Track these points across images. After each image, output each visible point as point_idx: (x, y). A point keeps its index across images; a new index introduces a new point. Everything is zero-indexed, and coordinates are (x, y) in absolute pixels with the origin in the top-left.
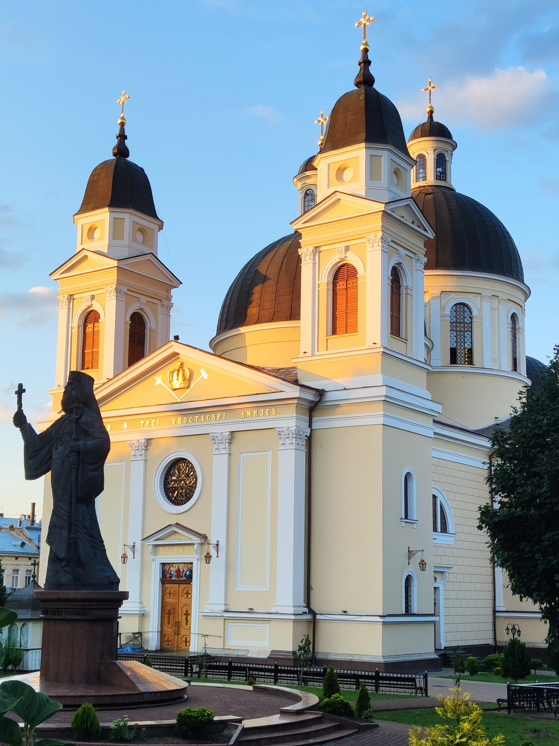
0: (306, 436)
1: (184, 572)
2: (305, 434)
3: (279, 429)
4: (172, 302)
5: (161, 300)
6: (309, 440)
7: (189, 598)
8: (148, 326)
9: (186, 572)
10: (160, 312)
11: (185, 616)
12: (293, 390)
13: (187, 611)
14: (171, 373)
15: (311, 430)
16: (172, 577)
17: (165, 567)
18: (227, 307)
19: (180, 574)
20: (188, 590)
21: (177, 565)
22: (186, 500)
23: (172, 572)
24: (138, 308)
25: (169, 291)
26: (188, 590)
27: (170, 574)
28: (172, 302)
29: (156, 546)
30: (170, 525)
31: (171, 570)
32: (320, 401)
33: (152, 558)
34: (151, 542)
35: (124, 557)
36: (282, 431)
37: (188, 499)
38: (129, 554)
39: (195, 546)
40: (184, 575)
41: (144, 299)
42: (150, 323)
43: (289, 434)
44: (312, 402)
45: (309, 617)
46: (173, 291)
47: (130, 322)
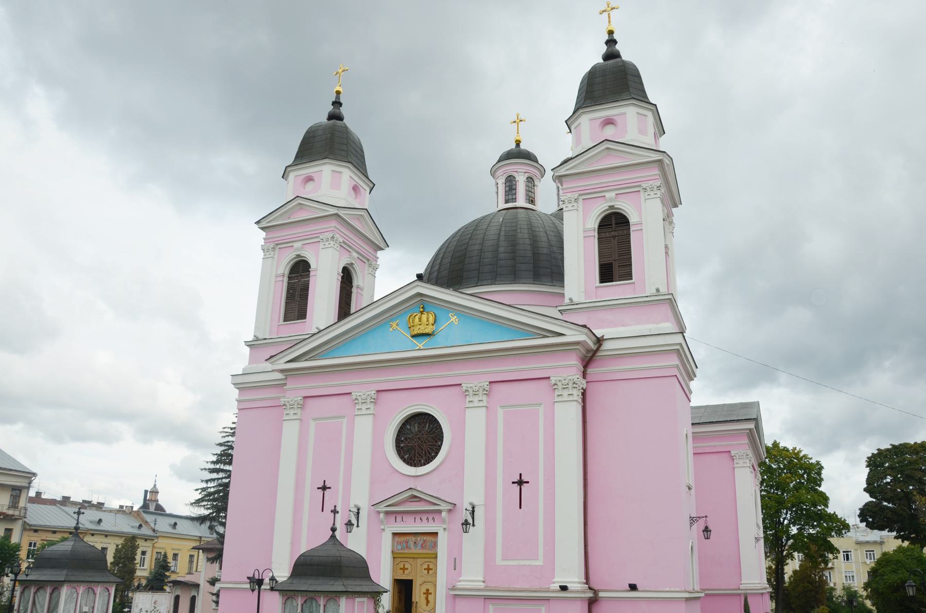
0: (582, 389)
2: (582, 386)
3: (555, 378)
4: (378, 263)
5: (368, 260)
6: (584, 394)
7: (430, 574)
8: (355, 283)
10: (367, 272)
12: (577, 333)
13: (428, 590)
14: (411, 317)
15: (587, 382)
18: (436, 273)
20: (428, 565)
22: (426, 461)
24: (349, 262)
25: (376, 251)
26: (428, 565)
28: (378, 263)
29: (387, 513)
30: (411, 488)
32: (598, 349)
33: (382, 527)
34: (382, 508)
35: (349, 524)
36: (560, 381)
37: (429, 460)
38: (354, 521)
39: (444, 514)
41: (355, 255)
42: (358, 280)
43: (568, 384)
44: (588, 351)
45: (591, 595)
46: (379, 254)
47: (342, 274)
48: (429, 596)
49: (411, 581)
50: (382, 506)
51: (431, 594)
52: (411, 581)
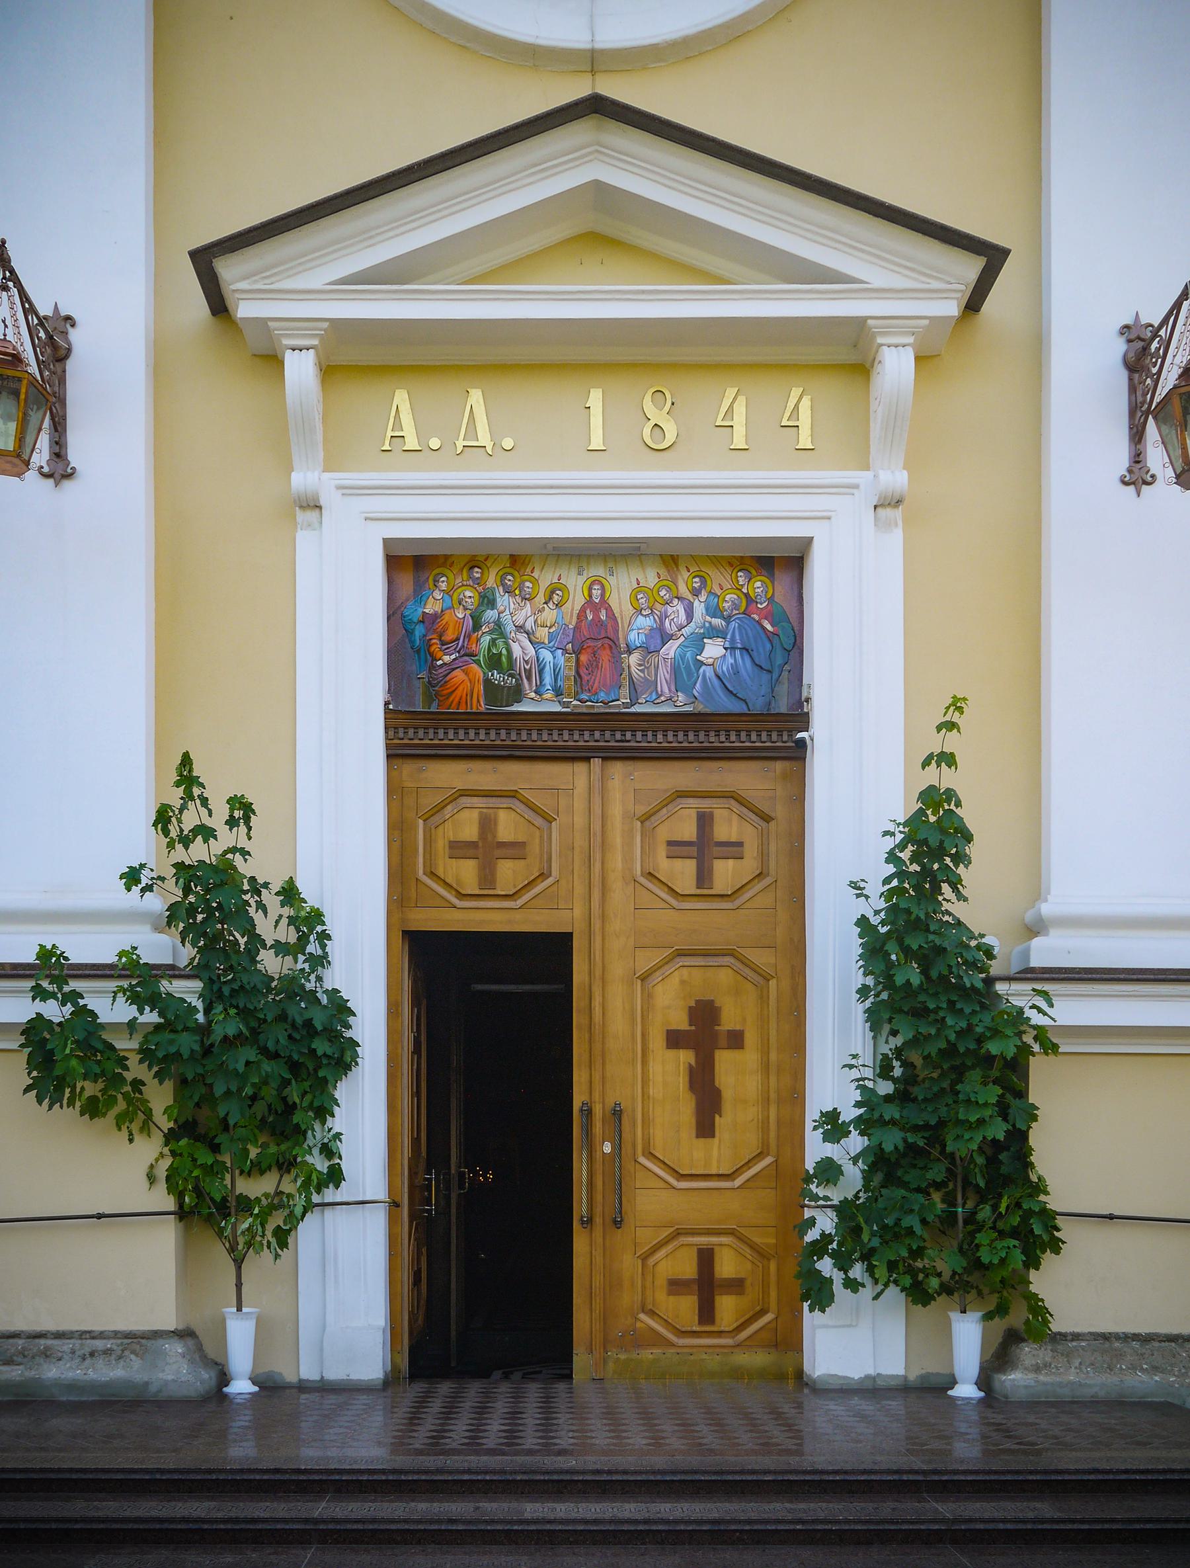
1: (671, 649)
9: (698, 642)
11: (686, 1057)
16: (517, 694)
17: (419, 593)
19: (617, 662)
20: (705, 821)
21: (576, 584)
23: (521, 649)
26: (705, 821)
27: (494, 662)
31: (498, 626)
40: (664, 674)
48: (724, 1060)
49: (567, 938)
50: (318, 278)
51: (736, 1040)
52: (567, 938)
